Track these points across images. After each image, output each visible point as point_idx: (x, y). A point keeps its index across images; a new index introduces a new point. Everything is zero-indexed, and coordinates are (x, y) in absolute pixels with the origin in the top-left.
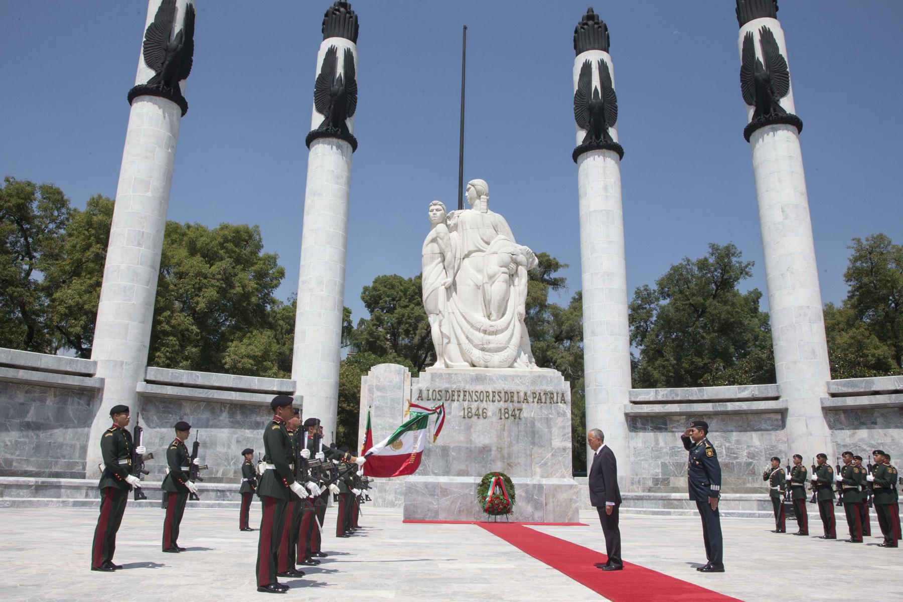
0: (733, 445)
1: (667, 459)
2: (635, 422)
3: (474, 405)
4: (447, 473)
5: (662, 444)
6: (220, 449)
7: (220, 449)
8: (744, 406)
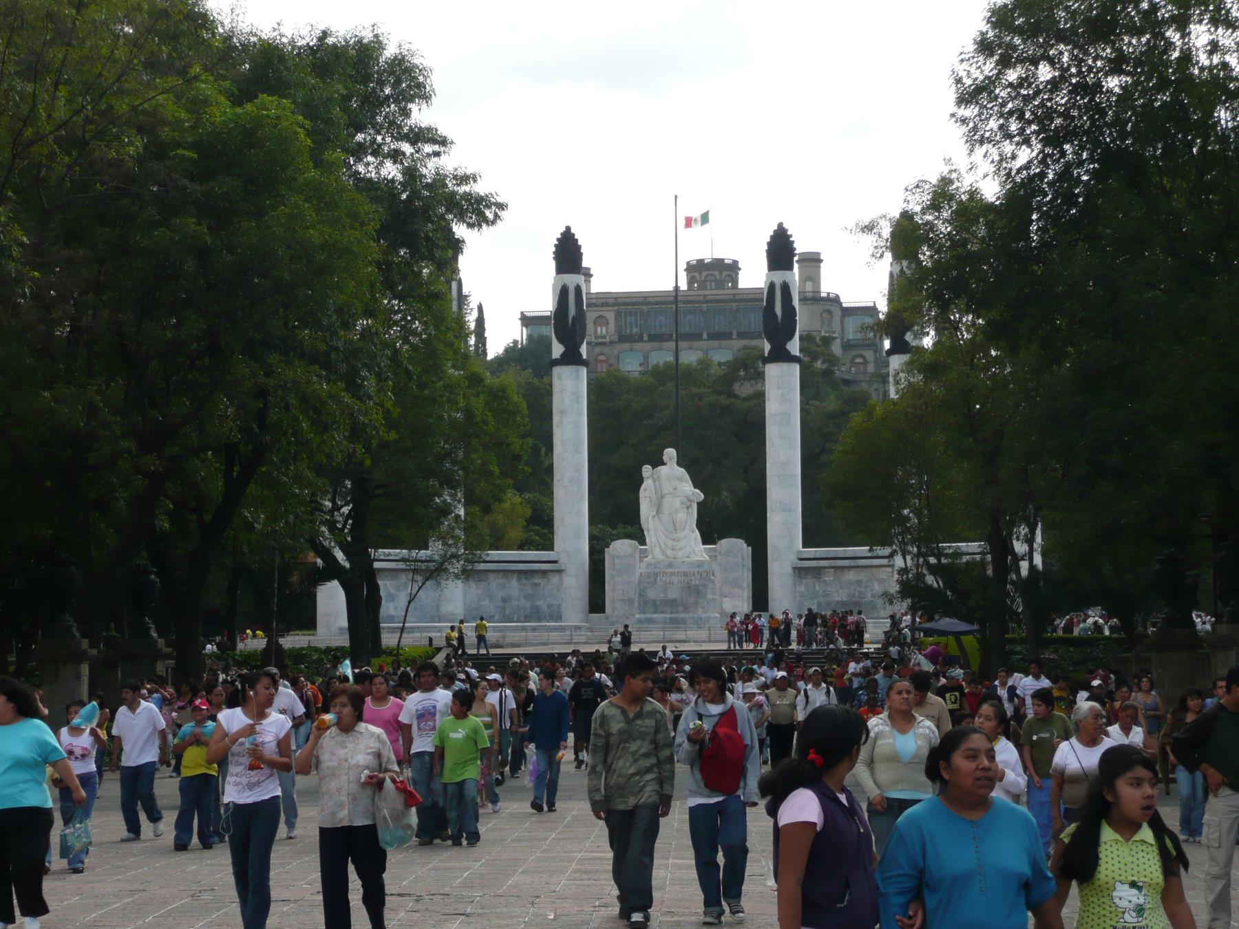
0: (862, 589)
1: (821, 599)
2: (801, 572)
3: (668, 579)
4: (656, 612)
5: (817, 588)
6: (514, 603)
7: (514, 603)
8: (868, 562)
